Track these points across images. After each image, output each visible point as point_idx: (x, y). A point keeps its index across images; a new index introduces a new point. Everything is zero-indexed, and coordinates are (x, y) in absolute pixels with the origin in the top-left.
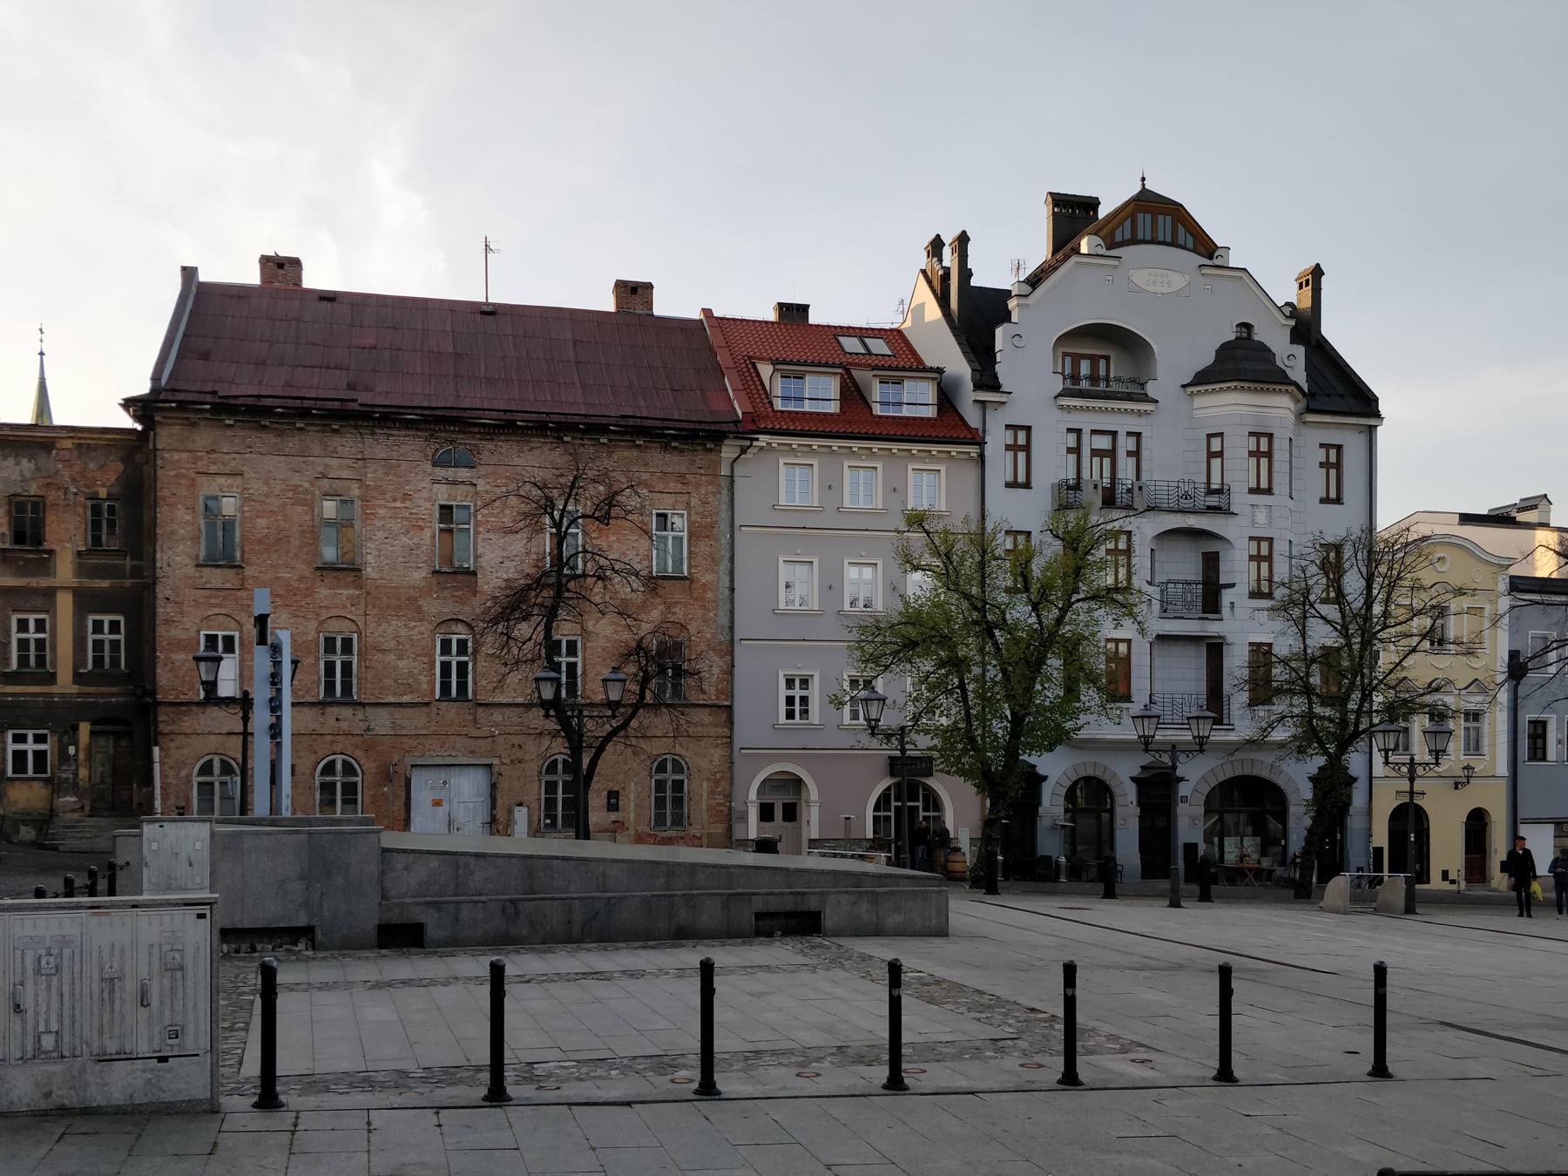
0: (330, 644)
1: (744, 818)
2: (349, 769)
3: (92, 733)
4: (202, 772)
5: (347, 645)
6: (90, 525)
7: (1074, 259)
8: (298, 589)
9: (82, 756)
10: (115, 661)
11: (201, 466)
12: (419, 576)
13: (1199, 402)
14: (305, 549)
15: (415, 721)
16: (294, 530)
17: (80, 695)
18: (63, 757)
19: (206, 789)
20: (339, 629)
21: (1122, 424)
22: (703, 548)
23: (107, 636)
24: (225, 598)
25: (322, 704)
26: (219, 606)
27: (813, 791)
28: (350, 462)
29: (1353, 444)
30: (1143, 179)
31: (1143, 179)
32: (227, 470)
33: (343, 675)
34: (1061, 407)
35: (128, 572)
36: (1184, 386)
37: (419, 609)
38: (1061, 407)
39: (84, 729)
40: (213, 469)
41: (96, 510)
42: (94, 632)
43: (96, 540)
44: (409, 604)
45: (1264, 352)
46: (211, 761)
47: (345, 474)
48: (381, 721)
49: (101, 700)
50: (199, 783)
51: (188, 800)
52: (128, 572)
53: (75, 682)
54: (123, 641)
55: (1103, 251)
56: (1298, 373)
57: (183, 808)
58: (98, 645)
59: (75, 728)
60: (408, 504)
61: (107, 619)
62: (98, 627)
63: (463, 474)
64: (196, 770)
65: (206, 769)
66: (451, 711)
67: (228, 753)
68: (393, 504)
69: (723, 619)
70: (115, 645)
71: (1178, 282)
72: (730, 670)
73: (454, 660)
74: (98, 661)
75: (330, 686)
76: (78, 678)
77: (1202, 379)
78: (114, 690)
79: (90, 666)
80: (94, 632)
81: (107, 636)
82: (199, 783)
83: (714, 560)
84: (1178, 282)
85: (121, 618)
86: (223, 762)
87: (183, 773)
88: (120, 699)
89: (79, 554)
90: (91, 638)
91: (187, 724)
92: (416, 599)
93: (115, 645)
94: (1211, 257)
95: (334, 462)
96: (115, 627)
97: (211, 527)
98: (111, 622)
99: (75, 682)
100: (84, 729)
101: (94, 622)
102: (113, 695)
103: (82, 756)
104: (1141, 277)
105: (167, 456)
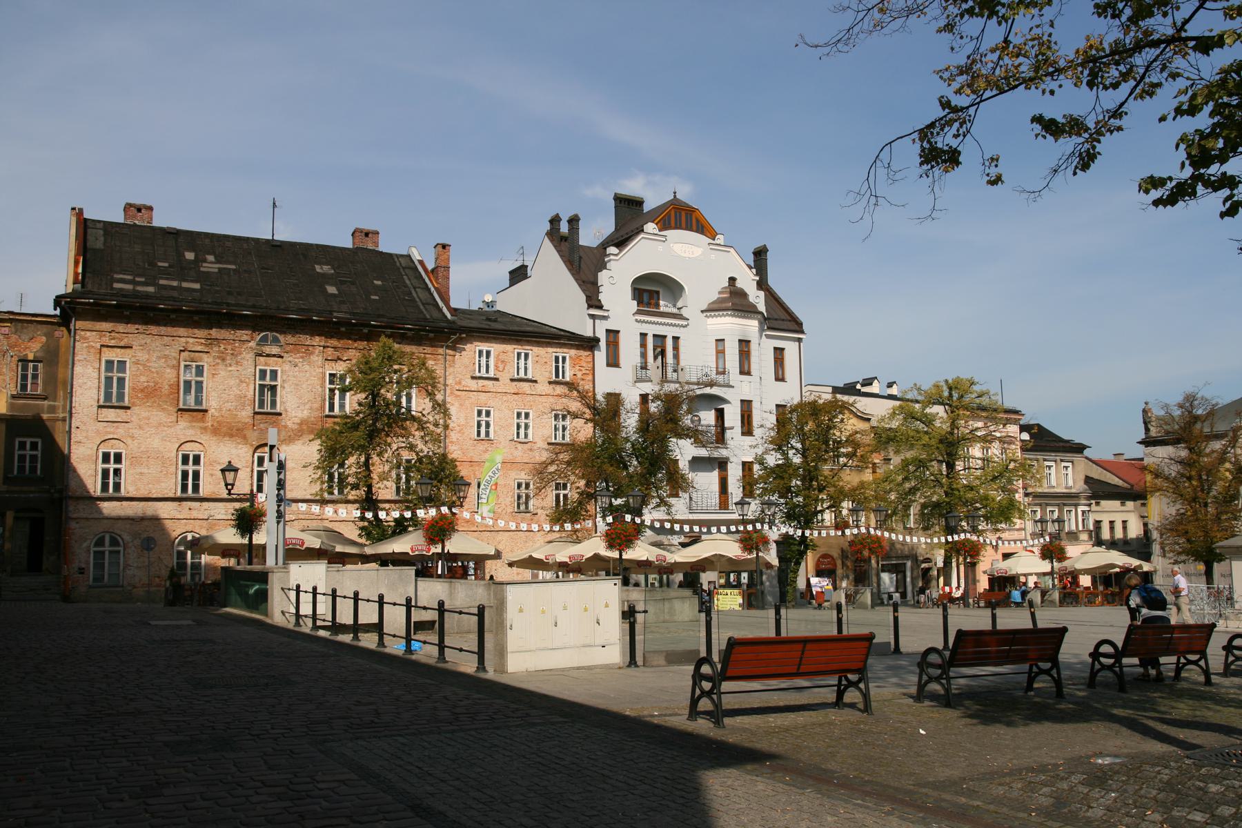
3: (16, 519)
4: (97, 545)
6: (19, 376)
7: (642, 235)
8: (166, 422)
9: (7, 534)
10: (33, 469)
11: (106, 341)
13: (710, 321)
14: (171, 396)
16: (165, 383)
17: (7, 492)
21: (670, 332)
23: (28, 452)
24: (117, 427)
26: (113, 433)
28: (203, 341)
29: (791, 349)
30: (675, 193)
31: (675, 193)
32: (122, 344)
33: (193, 480)
34: (636, 320)
35: (46, 409)
36: (702, 311)
37: (245, 437)
38: (636, 320)
39: (10, 516)
40: (112, 343)
42: (19, 449)
43: (24, 387)
45: (742, 294)
46: (104, 537)
47: (199, 348)
49: (23, 496)
50: (95, 552)
51: (88, 563)
52: (46, 409)
53: (4, 483)
54: (39, 455)
55: (656, 231)
56: (762, 307)
57: (83, 569)
58: (22, 458)
59: (3, 515)
60: (239, 368)
61: (28, 441)
62: (22, 446)
64: (93, 544)
65: (100, 542)
67: (116, 531)
68: (230, 369)
70: (34, 458)
74: (21, 468)
75: (184, 488)
77: (714, 309)
78: (33, 489)
79: (15, 472)
80: (19, 449)
81: (28, 452)
82: (95, 552)
85: (39, 441)
86: (112, 538)
87: (85, 545)
88: (37, 495)
89: (13, 397)
90: (17, 453)
92: (242, 430)
93: (34, 458)
94: (714, 240)
95: (191, 340)
96: (34, 446)
98: (31, 443)
99: (4, 483)
100: (10, 516)
101: (20, 442)
103: (7, 534)
104: (679, 249)
105: (83, 333)
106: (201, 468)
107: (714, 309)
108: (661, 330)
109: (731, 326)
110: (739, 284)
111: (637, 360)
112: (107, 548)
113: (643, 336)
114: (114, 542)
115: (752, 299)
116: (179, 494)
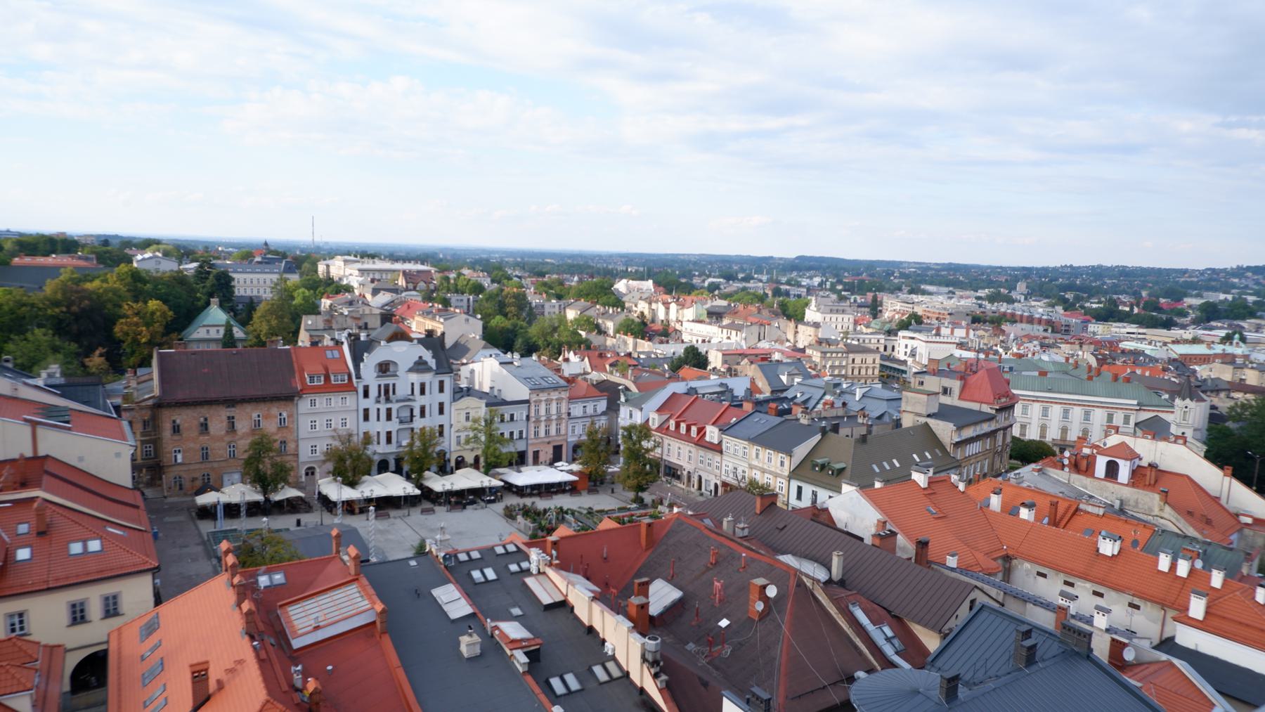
0: (203, 449)
1: (301, 477)
2: (208, 475)
5: (207, 449)
12: (223, 433)
15: (223, 464)
18: (139, 477)
19: (175, 482)
20: (205, 445)
22: (291, 419)
25: (202, 463)
27: (318, 470)
39: (144, 470)
41: (144, 422)
43: (145, 429)
44: (221, 439)
48: (215, 465)
63: (233, 409)
65: (175, 478)
66: (231, 461)
69: (296, 434)
71: (405, 349)
72: (297, 446)
73: (232, 449)
76: (142, 459)
83: (293, 422)
84: (405, 349)
91: (170, 469)
97: (174, 427)
100: (144, 470)
102: (151, 462)
106: (209, 451)
107: (411, 370)
108: (387, 382)
109: (415, 378)
110: (424, 358)
111: (376, 394)
112: (178, 479)
113: (380, 386)
114: (180, 478)
115: (430, 364)
116: (201, 460)
